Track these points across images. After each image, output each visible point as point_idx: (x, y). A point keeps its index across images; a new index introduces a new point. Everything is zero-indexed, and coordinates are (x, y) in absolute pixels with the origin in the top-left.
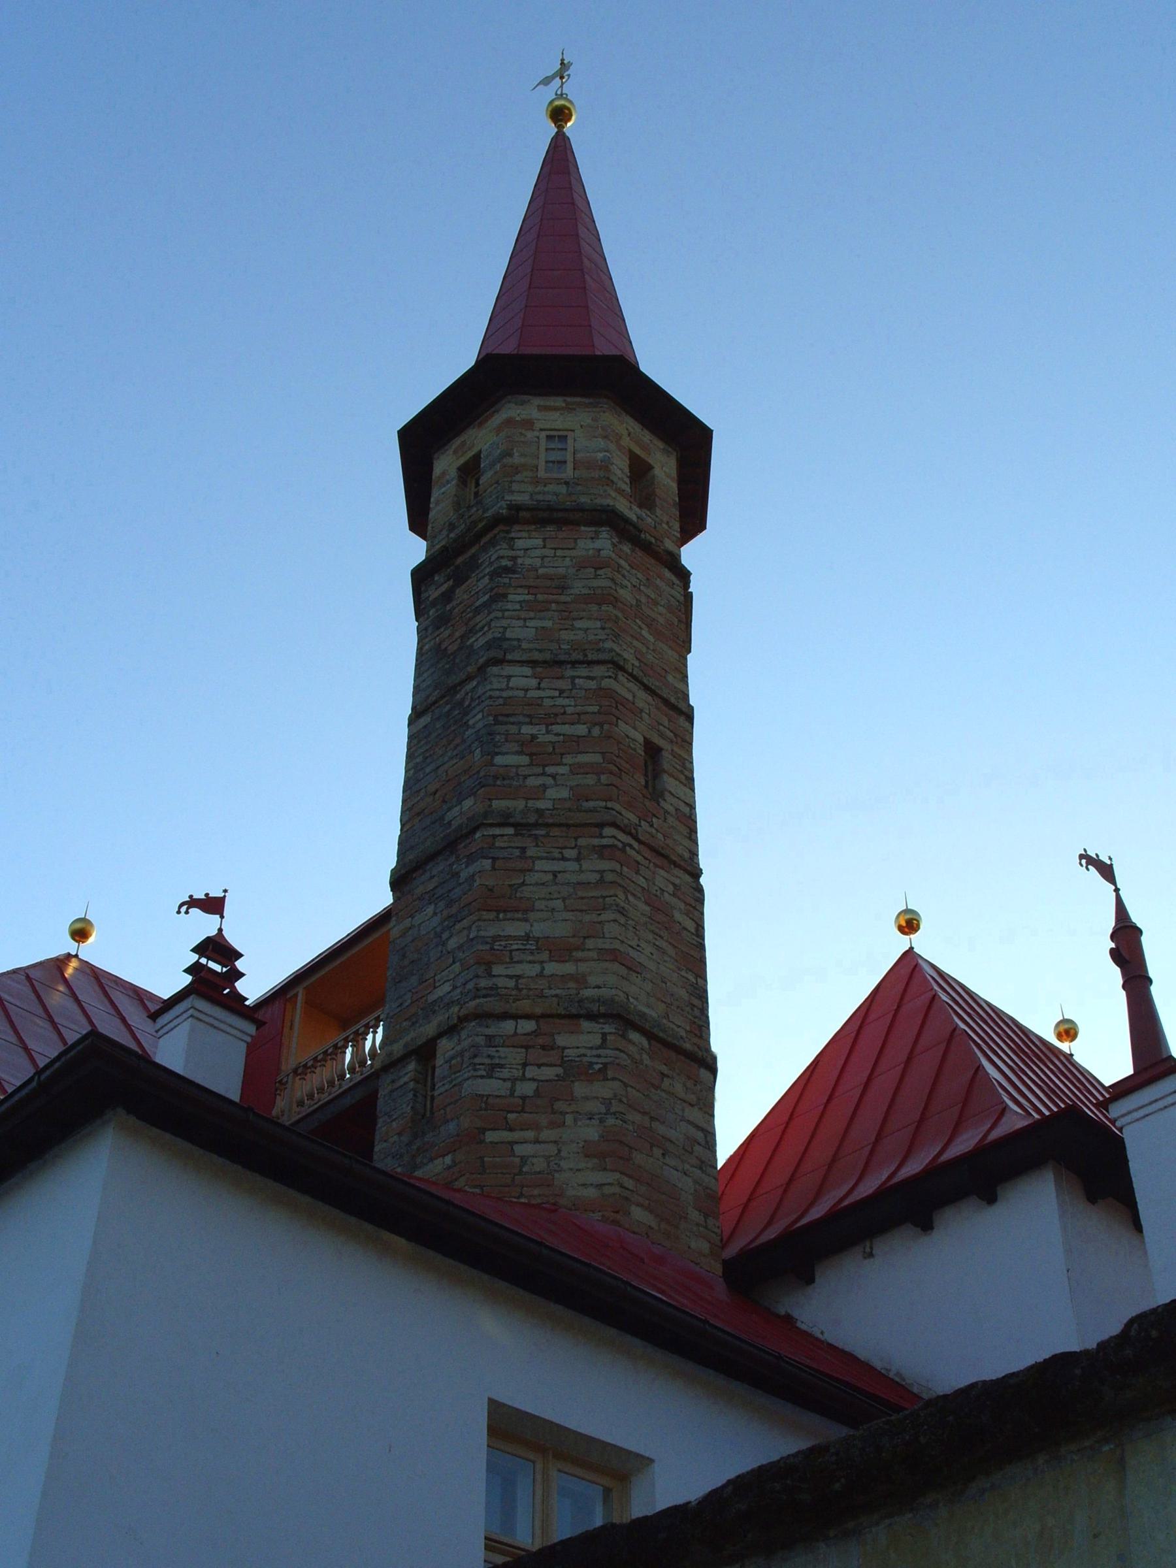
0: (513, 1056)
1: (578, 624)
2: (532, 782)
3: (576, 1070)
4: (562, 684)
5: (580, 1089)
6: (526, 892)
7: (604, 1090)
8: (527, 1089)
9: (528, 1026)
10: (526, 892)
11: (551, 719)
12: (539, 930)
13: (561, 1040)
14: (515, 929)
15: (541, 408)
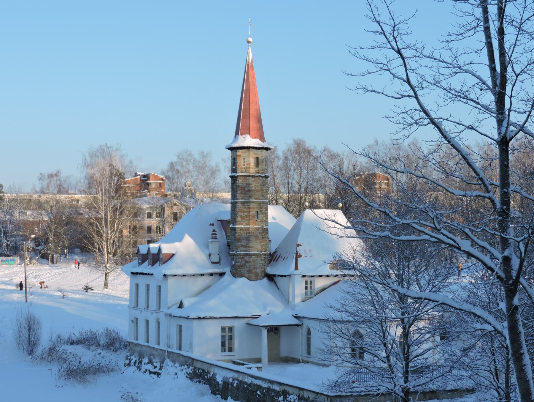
0: (240, 260)
1: (247, 196)
2: (242, 222)
3: (246, 262)
4: (245, 207)
5: (247, 264)
6: (241, 239)
7: (249, 264)
8: (242, 264)
9: (242, 256)
10: (241, 239)
11: (243, 212)
12: (243, 244)
13: (245, 258)
14: (240, 244)
15: (242, 152)
